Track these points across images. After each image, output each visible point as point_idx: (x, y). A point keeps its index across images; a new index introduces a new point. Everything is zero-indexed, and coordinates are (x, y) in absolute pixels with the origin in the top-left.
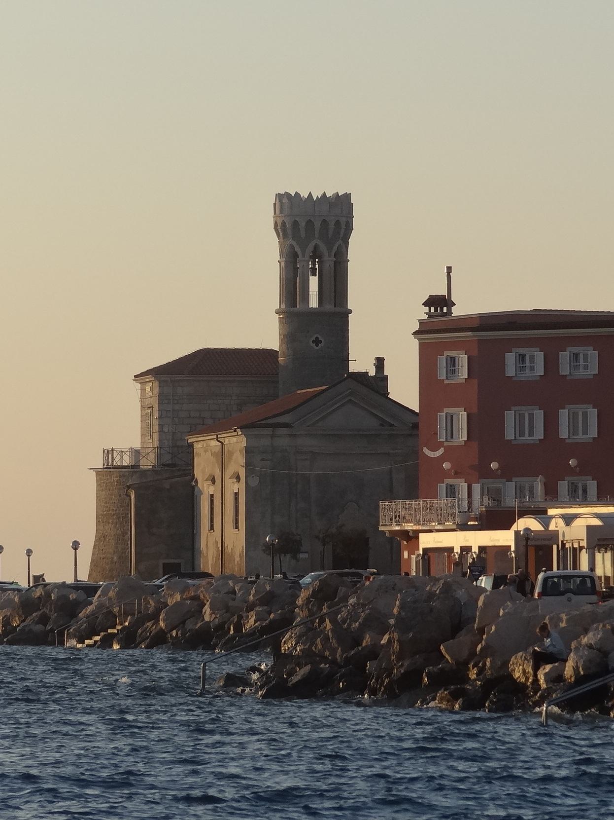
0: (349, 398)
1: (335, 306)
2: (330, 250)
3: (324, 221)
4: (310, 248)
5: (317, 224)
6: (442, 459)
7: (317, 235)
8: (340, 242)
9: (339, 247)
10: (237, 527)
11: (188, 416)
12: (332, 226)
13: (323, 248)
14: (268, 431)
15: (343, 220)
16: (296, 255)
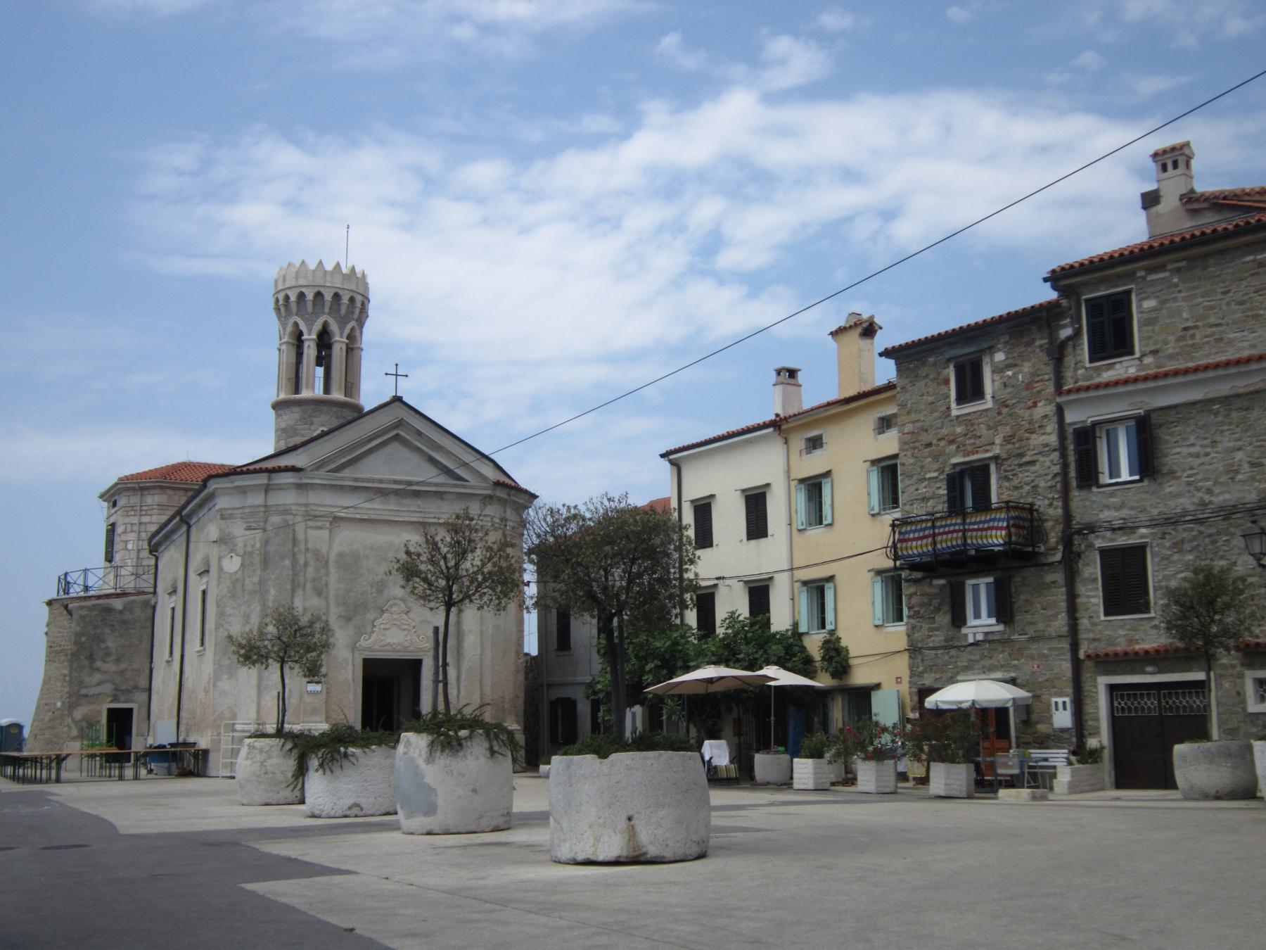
2: (342, 329)
4: (318, 326)
5: (328, 297)
7: (327, 310)
8: (353, 324)
9: (353, 329)
12: (345, 300)
13: (334, 327)
15: (359, 299)
16: (301, 334)
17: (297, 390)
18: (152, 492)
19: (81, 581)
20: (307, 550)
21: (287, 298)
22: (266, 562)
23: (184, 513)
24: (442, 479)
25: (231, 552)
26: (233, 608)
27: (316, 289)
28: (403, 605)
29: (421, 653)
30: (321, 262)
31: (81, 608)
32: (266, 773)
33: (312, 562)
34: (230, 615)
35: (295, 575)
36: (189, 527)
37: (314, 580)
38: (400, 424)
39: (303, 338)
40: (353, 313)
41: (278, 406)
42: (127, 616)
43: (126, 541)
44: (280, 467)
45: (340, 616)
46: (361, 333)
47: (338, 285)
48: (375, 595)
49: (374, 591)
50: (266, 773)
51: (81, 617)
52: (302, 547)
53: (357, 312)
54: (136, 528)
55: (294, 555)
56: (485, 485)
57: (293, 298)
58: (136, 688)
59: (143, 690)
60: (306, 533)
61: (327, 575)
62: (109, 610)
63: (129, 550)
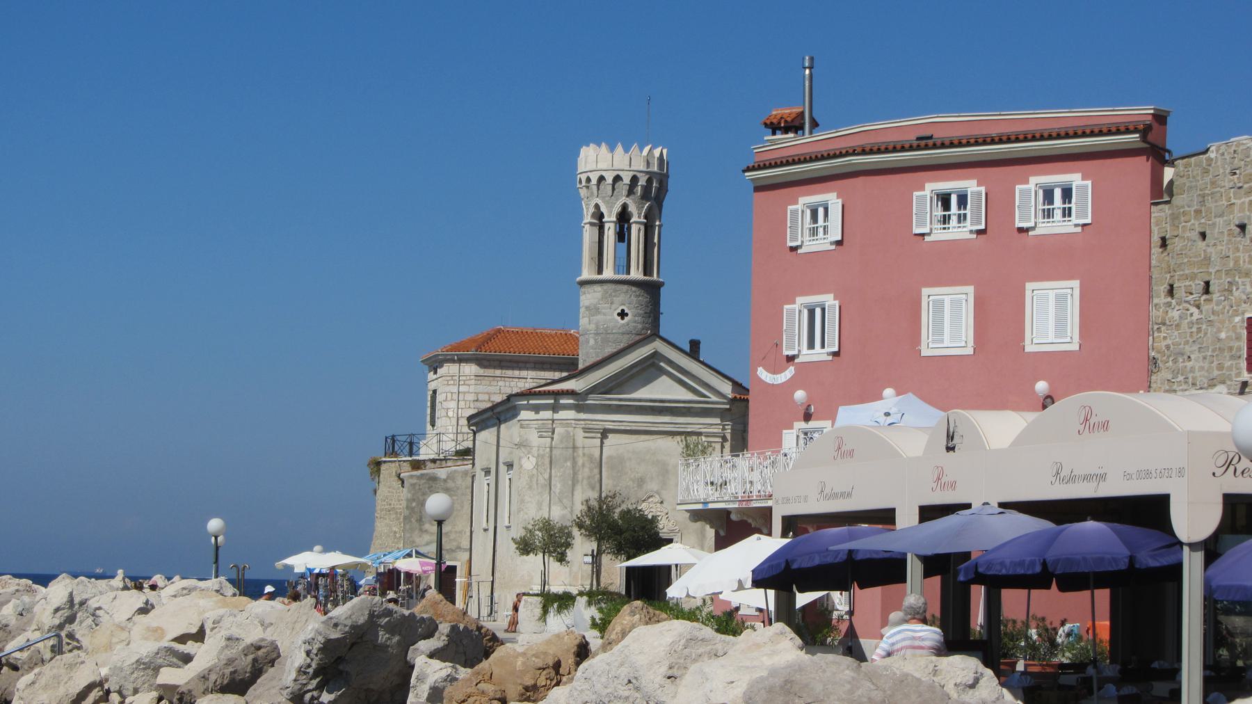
2: (640, 209)
4: (617, 208)
5: (627, 180)
6: (791, 385)
9: (650, 208)
11: (476, 399)
13: (632, 208)
16: (601, 216)
17: (600, 271)
23: (495, 411)
24: (690, 396)
25: (528, 454)
26: (530, 497)
27: (616, 173)
28: (657, 496)
29: (671, 534)
31: (412, 476)
32: (534, 616)
33: (587, 465)
34: (527, 503)
35: (575, 474)
37: (589, 478)
38: (656, 355)
39: (603, 220)
42: (450, 484)
43: (448, 409)
44: (563, 391)
47: (635, 169)
48: (636, 489)
49: (635, 485)
50: (534, 616)
51: (412, 485)
54: (455, 397)
55: (574, 458)
56: (725, 401)
57: (594, 181)
58: (459, 548)
59: (465, 550)
62: (434, 479)
63: (450, 418)
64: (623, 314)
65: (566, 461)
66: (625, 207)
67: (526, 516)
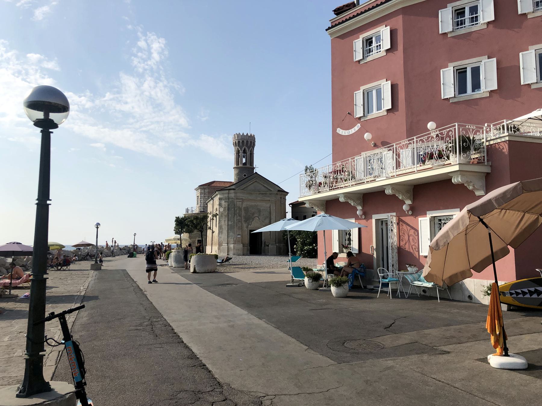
0: (256, 180)
1: (250, 166)
2: (249, 149)
3: (247, 141)
4: (243, 149)
5: (245, 142)
6: (360, 133)
7: (245, 145)
9: (251, 149)
10: (216, 227)
12: (249, 143)
13: (247, 149)
14: (227, 191)
16: (239, 151)
18: (206, 189)
19: (191, 209)
20: (237, 206)
21: (236, 142)
22: (228, 209)
30: (243, 133)
36: (213, 200)
40: (251, 145)
41: (234, 168)
45: (244, 221)
46: (254, 149)
52: (236, 206)
53: (252, 145)
54: (203, 197)
60: (237, 203)
61: (241, 212)
64: (245, 175)
65: (232, 209)
66: (245, 149)
67: (221, 225)
